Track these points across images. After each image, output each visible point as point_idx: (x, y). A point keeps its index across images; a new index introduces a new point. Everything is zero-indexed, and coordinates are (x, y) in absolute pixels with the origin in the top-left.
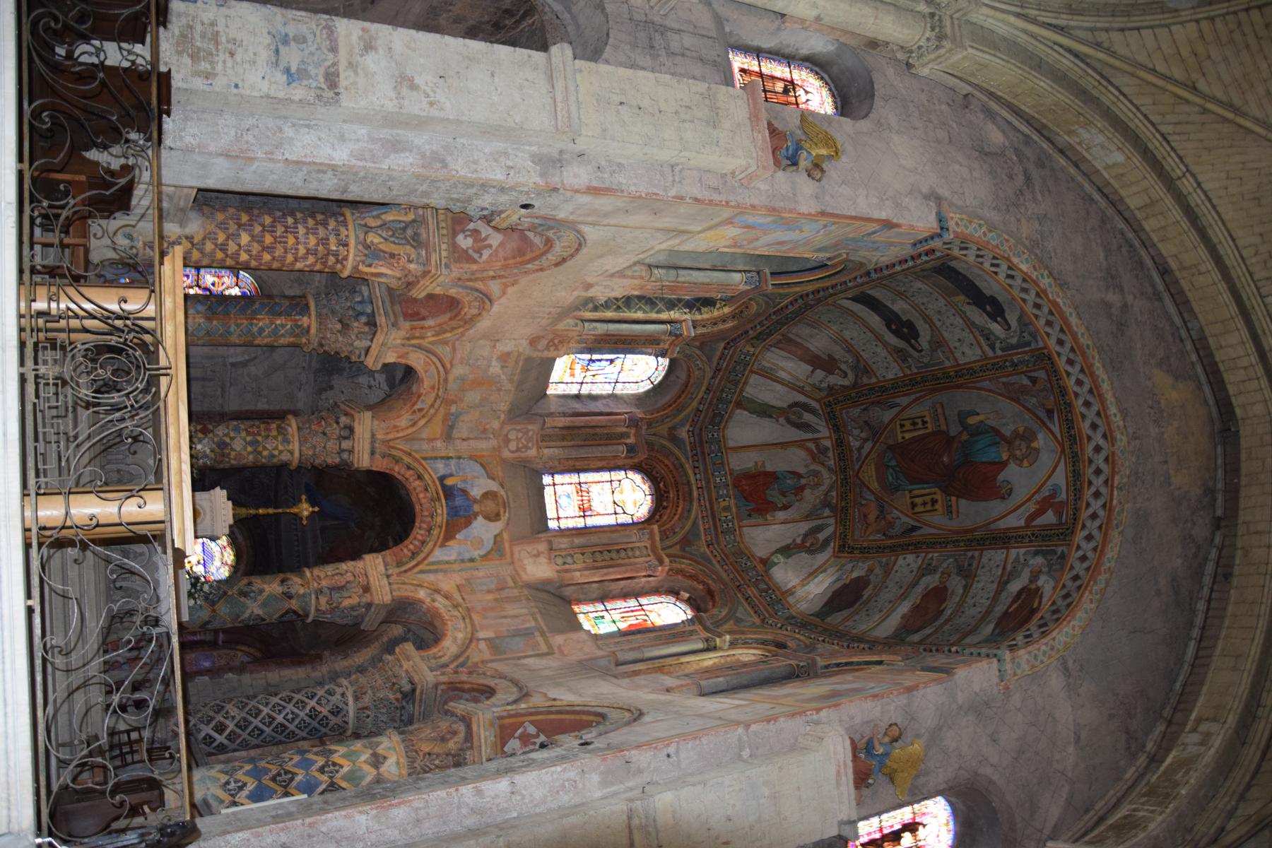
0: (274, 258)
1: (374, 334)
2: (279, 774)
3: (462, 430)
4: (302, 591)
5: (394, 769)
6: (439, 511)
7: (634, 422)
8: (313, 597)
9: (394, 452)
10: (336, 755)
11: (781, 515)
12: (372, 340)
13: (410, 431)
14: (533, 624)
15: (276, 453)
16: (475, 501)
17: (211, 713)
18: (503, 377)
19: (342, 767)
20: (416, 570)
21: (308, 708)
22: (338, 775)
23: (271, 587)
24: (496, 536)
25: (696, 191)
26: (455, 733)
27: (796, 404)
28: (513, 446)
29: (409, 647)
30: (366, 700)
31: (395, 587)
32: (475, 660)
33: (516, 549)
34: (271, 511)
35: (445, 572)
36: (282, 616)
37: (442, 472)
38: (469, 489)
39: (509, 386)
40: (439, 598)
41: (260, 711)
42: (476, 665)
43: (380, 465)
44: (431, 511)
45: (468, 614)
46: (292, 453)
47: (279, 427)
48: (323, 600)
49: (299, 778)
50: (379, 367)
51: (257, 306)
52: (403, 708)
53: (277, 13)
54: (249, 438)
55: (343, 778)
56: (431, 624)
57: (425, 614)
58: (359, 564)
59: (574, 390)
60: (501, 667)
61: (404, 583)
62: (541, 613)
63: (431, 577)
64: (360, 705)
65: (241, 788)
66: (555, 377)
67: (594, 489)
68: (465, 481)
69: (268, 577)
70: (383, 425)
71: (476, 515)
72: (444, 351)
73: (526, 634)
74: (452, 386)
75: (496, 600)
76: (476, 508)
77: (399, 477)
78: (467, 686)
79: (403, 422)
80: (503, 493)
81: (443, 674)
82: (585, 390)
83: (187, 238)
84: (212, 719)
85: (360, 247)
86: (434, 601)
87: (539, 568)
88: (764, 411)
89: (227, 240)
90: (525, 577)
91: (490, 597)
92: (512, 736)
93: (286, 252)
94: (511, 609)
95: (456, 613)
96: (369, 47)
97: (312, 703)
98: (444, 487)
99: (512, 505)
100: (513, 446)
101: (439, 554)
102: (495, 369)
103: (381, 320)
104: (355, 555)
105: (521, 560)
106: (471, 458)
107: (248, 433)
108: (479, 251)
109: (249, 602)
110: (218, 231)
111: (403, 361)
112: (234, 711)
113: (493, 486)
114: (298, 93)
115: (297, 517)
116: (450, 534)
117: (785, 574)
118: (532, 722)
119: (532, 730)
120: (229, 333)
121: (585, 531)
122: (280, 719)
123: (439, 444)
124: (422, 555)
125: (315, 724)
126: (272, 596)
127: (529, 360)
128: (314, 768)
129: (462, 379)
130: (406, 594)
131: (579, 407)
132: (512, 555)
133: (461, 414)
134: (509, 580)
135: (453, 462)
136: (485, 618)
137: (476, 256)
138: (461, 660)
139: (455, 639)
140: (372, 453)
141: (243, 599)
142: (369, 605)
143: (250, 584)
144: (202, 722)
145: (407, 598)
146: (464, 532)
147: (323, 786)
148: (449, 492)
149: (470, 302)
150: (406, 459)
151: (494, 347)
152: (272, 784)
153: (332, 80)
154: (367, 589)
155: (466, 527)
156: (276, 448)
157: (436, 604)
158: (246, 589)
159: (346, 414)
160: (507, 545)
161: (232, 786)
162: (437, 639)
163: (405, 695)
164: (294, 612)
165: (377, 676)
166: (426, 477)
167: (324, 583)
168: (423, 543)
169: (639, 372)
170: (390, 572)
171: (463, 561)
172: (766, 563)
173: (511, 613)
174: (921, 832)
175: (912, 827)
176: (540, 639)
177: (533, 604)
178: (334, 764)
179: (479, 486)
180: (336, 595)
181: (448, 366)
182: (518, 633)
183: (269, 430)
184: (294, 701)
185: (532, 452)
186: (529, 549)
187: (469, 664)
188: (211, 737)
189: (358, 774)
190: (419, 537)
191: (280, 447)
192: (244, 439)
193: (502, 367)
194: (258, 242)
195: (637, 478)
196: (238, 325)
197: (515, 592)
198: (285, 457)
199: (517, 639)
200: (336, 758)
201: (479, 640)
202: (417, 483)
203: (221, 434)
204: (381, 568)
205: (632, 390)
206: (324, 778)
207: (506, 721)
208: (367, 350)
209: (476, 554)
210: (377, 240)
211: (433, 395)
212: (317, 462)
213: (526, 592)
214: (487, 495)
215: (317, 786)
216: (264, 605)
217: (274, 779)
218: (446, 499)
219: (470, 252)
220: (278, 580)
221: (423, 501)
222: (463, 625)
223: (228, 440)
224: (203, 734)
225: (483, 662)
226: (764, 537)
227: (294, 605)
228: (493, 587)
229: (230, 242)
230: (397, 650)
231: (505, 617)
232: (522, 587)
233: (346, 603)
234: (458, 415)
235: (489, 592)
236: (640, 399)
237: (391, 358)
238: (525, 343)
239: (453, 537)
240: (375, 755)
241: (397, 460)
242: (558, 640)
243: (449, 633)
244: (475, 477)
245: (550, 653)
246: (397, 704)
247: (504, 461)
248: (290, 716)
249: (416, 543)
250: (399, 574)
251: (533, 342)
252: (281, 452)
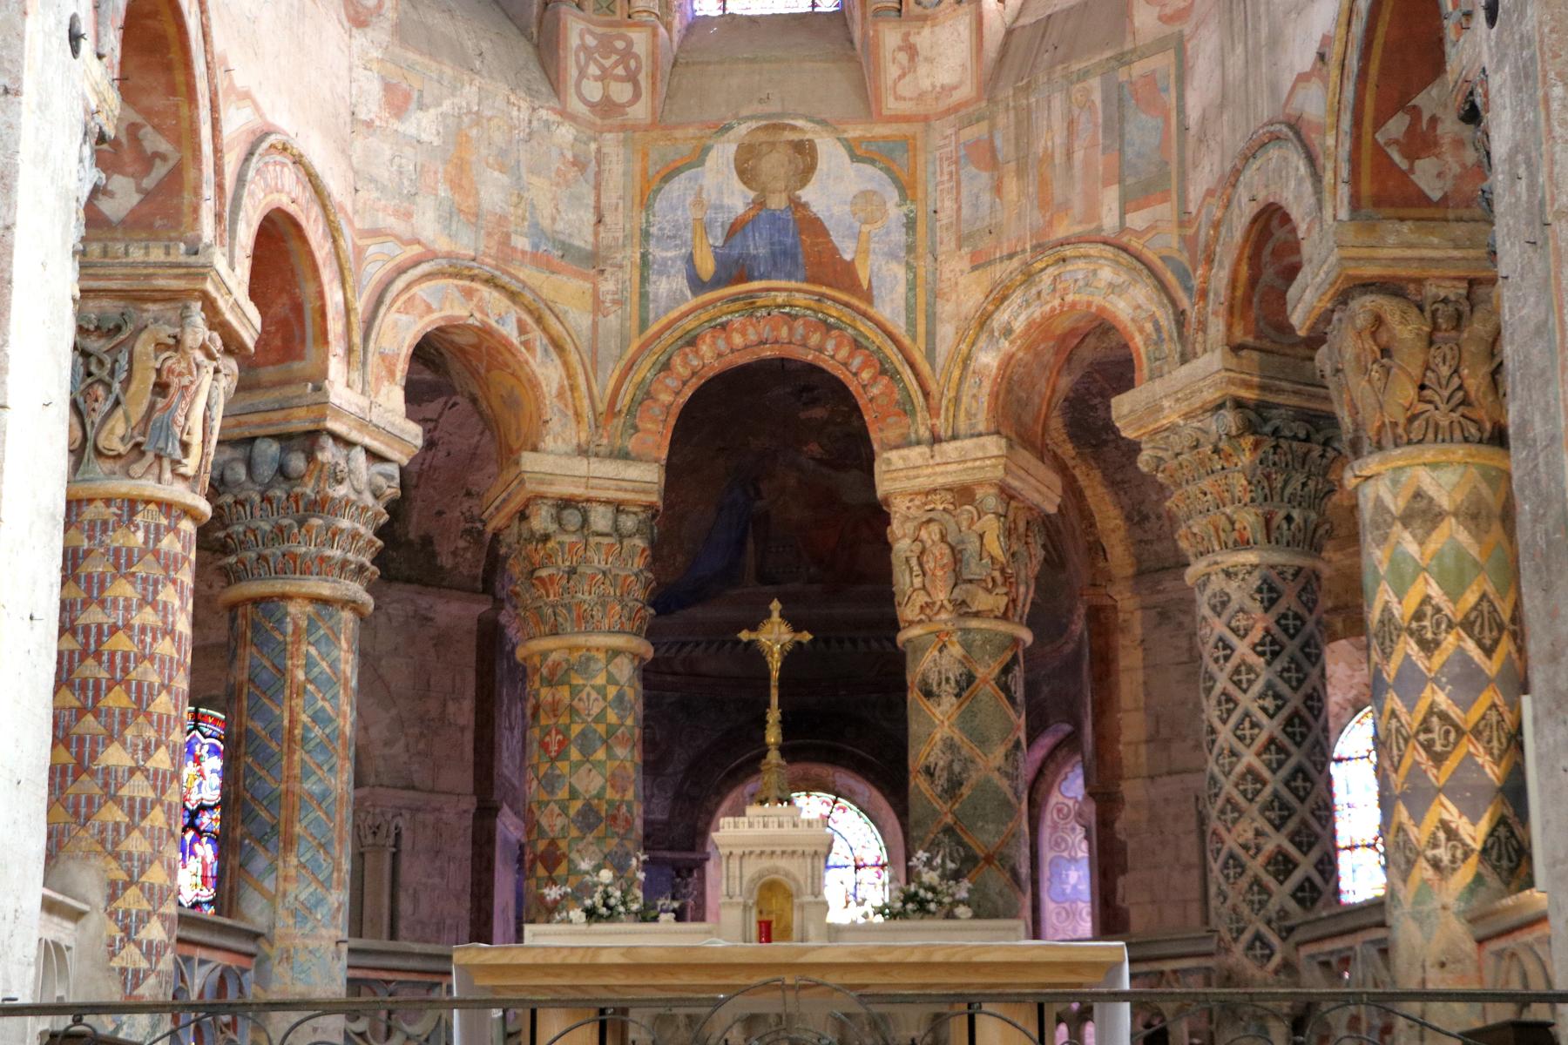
0: (166, 687)
1: (337, 438)
2: (1428, 746)
3: (576, 224)
4: (956, 650)
5: (1449, 477)
6: (781, 298)
8: (974, 623)
9: (624, 401)
10: (1397, 610)
12: (349, 444)
13: (574, 358)
14: (1095, 83)
15: (612, 691)
16: (759, 204)
17: (1244, 882)
18: (446, 106)
19: (1427, 599)
20: (925, 368)
21: (1254, 659)
22: (1447, 608)
23: (935, 727)
24: (855, 158)
26: (1378, 321)
28: (621, 92)
30: (1248, 519)
31: (963, 426)
32: (1174, 242)
33: (891, 105)
34: (774, 715)
35: (935, 295)
36: (1012, 700)
37: (681, 283)
38: (727, 218)
39: (469, 93)
40: (1002, 317)
41: (1250, 770)
42: (1188, 242)
43: (656, 435)
44: (776, 322)
45: (1054, 250)
46: (614, 653)
47: (550, 682)
48: (983, 601)
49: (1443, 701)
50: (414, 433)
51: (257, 726)
52: (1276, 432)
54: (575, 754)
55: (1454, 597)
56: (1063, 338)
57: (1037, 355)
58: (900, 509)
60: (1203, 178)
61: (957, 400)
62: (1066, 59)
63: (946, 333)
64: (1261, 537)
65: (1452, 834)
68: (706, 227)
69: (913, 727)
70: (555, 425)
71: (797, 205)
74: (465, 244)
75: (1021, 173)
76: (777, 202)
77: (688, 393)
78: (1244, 270)
80: (743, 129)
81: (1203, 326)
83: (113, 897)
84: (1257, 881)
85: (137, 469)
86: (1007, 331)
89: (118, 801)
90: (966, 91)
91: (1011, 186)
92: (1404, 175)
93: (152, 658)
94: (1050, 136)
95: (1046, 279)
97: (1242, 648)
98: (718, 281)
99: (774, 107)
100: (621, 92)
101: (890, 307)
102: (424, 125)
103: (300, 421)
104: (878, 515)
105: (921, 96)
106: (646, 204)
107: (562, 754)
108: (148, 161)
109: (974, 777)
110: (95, 823)
111: (402, 367)
112: (1244, 831)
113: (723, 154)
115: (793, 656)
116: (835, 273)
118: (1379, 123)
119: (1397, 126)
120: (325, 795)
122: (1271, 727)
123: (608, 286)
124: (890, 350)
125: (1292, 646)
126: (966, 720)
127: (401, 32)
128: (1422, 664)
129: (450, 215)
130: (985, 399)
132: (907, 119)
133: (535, 225)
134: (969, 134)
135: (657, 253)
136: (1065, 207)
137: (160, 170)
138: (1170, 277)
139: (1112, 286)
141: (966, 791)
142: (1007, 494)
143: (929, 772)
144: (1262, 904)
145: (995, 396)
146: (835, 238)
147: (1470, 646)
148: (734, 270)
149: (269, 190)
150: (644, 370)
151: (369, 124)
152: (1450, 764)
154: (964, 494)
155: (824, 232)
156: (601, 691)
157: (1019, 325)
158: (942, 780)
159: (523, 516)
160: (880, 130)
161: (1443, 854)
162: (1103, 327)
163: (1249, 427)
164: (1006, 670)
165: (1192, 489)
166: (689, 323)
167: (941, 596)
168: (857, 345)
170: (924, 433)
171: (911, 249)
173: (1058, 141)
176: (1139, 68)
177: (1042, 78)
178: (1419, 616)
179: (720, 189)
180: (974, 569)
181: (416, 250)
182: (1115, 126)
183: (554, 709)
184: (1232, 689)
186: (893, 71)
187: (1184, 258)
188: (1301, 888)
189: (1449, 561)
190: (843, 353)
191: (600, 680)
192: (576, 766)
193: (422, 107)
194: (124, 724)
196: (307, 774)
197: (1005, 120)
198: (624, 670)
199: (1132, 131)
200: (1402, 611)
201: (1123, 228)
202: (704, 348)
203: (560, 822)
204: (915, 454)
206: (1449, 641)
207: (1366, 187)
208: (374, 456)
209: (895, 212)
210: (118, 426)
211: (486, 292)
212: (638, 592)
213: (1006, 92)
214: (746, 173)
215: (1467, 660)
216: (983, 742)
217: (1438, 759)
218: (750, 278)
219: (148, 183)
220: (927, 705)
221: (752, 337)
222: (1081, 264)
223: (577, 805)
224: (1292, 905)
225: (1182, 224)
227: (987, 670)
228: (985, 177)
229: (125, 792)
230: (1128, 434)
231: (1069, 154)
232: (992, 100)
233: (995, 546)
234: (537, 232)
235: (998, 189)
237: (393, 397)
238: (360, 39)
239: (850, 266)
240: (1407, 519)
241: (646, 395)
243: (1098, 300)
244: (698, 202)
245: (1180, 47)
246: (1267, 445)
247: (658, 122)
248: (1269, 703)
249: (856, 363)
250: (933, 411)
252: (611, 680)
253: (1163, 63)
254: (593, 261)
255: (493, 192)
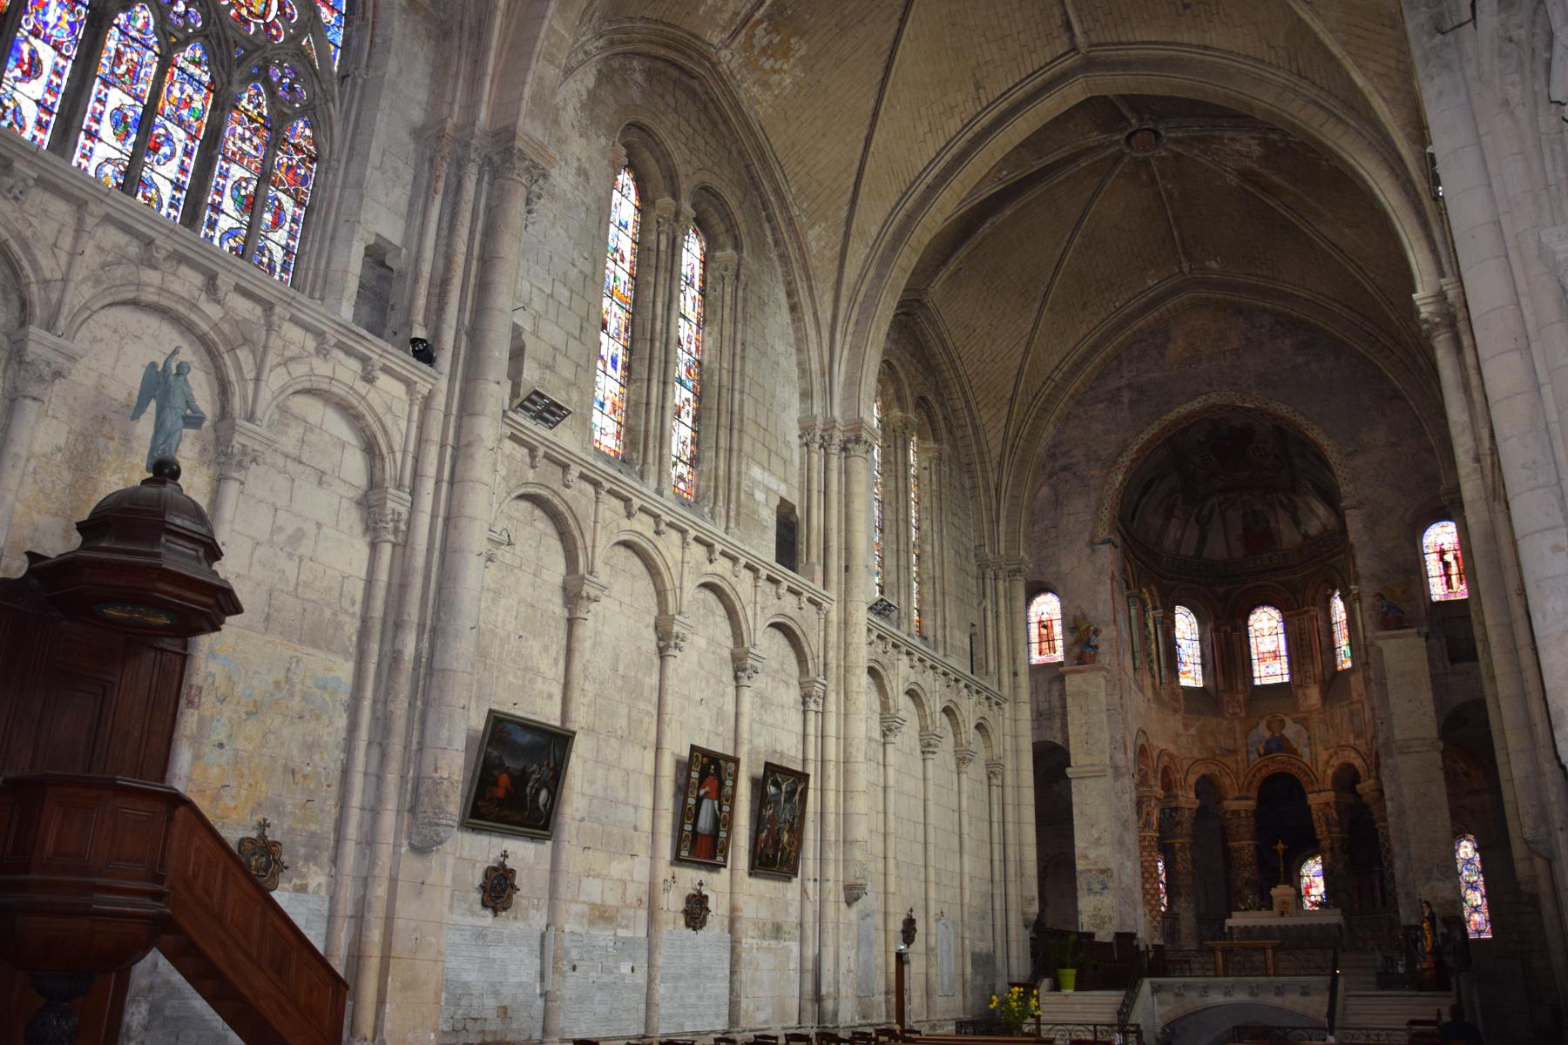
7: (1216, 629)
11: (1273, 524)
25: (1117, 698)
27: (1197, 521)
29: (1358, 787)
43: (1254, 793)
53: (1080, 893)
59: (1199, 668)
66: (1191, 684)
67: (1262, 649)
72: (1186, 764)
73: (1351, 713)
79: (1227, 781)
82: (1198, 660)
87: (1314, 695)
88: (1203, 539)
96: (1086, 857)
101: (1306, 759)
102: (1193, 731)
103: (1174, 805)
104: (1309, 808)
113: (1263, 723)
114: (1110, 884)
115: (1285, 851)
116: (1294, 751)
117: (1314, 527)
121: (1289, 655)
131: (1210, 667)
140: (1247, 798)
148: (1268, 751)
153: (1103, 872)
154: (1327, 804)
169: (1186, 625)
172: (1306, 536)
174: (1446, 547)
175: (1442, 553)
185: (1241, 697)
195: (1252, 618)
205: (1195, 626)
214: (1269, 728)
226: (1288, 535)
236: (1201, 623)
237: (1192, 795)
241: (1251, 783)
242: (1355, 695)
251: (1176, 711)
253: (1358, 706)
254: (1234, 752)
255: (1210, 742)
